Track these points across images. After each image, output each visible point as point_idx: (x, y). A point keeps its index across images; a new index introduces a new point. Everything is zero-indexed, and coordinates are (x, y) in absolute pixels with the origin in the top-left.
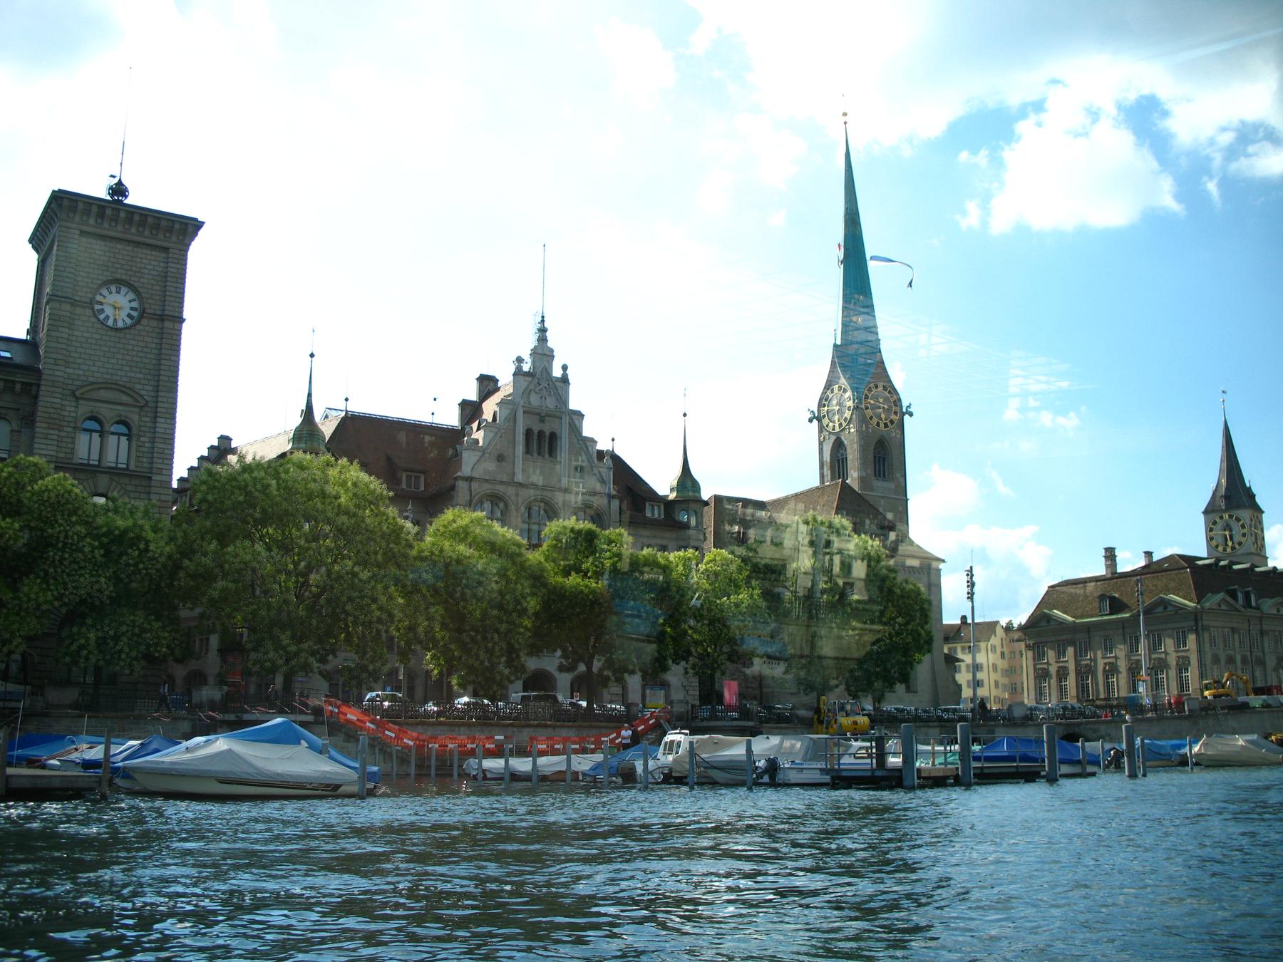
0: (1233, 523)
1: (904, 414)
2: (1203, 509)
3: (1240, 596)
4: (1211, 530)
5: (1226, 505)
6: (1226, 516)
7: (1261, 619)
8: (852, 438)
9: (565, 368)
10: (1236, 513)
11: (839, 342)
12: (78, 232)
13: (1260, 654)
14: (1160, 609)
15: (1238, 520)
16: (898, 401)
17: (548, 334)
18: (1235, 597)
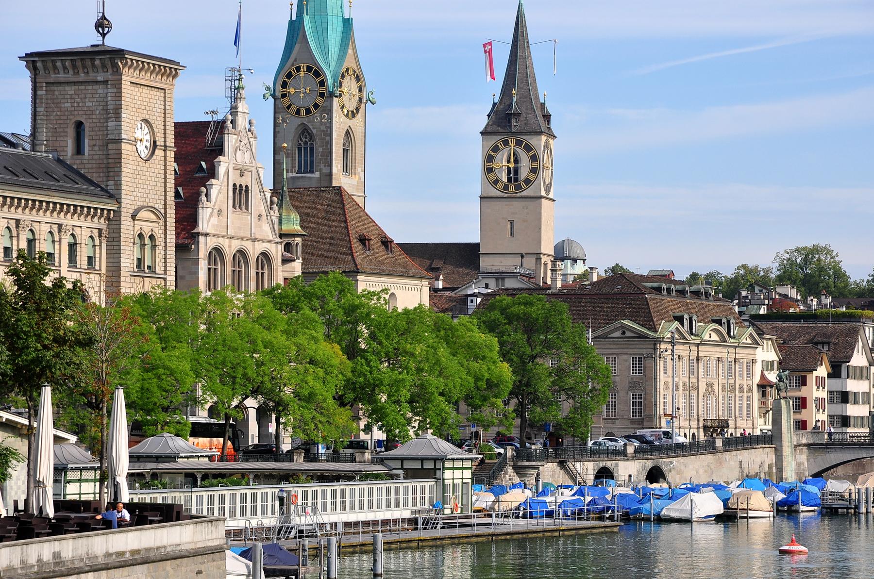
2: (482, 129)
4: (490, 159)
7: (698, 345)
8: (323, 128)
14: (618, 334)
15: (528, 148)
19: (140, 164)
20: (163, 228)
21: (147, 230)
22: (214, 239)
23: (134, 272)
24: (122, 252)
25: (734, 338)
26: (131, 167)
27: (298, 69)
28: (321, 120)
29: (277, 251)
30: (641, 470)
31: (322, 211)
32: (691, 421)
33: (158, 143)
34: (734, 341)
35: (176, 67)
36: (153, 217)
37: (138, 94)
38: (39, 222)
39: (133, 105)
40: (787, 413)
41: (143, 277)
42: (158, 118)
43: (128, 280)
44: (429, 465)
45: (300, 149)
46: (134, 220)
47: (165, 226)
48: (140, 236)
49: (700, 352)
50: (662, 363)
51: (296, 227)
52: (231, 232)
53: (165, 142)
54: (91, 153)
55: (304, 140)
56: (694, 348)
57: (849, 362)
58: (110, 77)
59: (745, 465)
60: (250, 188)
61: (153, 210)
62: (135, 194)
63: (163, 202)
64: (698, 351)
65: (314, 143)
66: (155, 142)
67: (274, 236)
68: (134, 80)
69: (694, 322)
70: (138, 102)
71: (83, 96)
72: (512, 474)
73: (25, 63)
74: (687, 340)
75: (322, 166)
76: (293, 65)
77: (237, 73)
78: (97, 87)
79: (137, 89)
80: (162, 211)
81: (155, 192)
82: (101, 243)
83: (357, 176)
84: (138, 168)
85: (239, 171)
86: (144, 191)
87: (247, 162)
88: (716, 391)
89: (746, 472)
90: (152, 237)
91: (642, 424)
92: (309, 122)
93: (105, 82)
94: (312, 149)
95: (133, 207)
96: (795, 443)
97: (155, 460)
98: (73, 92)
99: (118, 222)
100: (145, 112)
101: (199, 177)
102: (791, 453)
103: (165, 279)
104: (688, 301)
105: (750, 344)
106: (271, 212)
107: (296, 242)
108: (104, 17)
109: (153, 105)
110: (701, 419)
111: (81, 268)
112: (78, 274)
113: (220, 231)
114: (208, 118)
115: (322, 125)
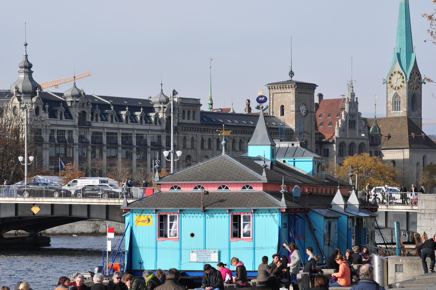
1: (422, 83)
8: (404, 94)
9: (357, 98)
16: (420, 78)
22: (342, 139)
27: (395, 73)
31: (399, 125)
37: (301, 96)
39: (299, 99)
52: (348, 137)
55: (397, 98)
58: (291, 91)
60: (356, 121)
61: (307, 132)
66: (308, 111)
68: (299, 91)
70: (301, 98)
71: (284, 97)
75: (403, 108)
76: (393, 71)
79: (301, 94)
87: (355, 112)
92: (399, 92)
100: (304, 101)
101: (337, 118)
108: (291, 71)
109: (307, 99)
114: (341, 97)
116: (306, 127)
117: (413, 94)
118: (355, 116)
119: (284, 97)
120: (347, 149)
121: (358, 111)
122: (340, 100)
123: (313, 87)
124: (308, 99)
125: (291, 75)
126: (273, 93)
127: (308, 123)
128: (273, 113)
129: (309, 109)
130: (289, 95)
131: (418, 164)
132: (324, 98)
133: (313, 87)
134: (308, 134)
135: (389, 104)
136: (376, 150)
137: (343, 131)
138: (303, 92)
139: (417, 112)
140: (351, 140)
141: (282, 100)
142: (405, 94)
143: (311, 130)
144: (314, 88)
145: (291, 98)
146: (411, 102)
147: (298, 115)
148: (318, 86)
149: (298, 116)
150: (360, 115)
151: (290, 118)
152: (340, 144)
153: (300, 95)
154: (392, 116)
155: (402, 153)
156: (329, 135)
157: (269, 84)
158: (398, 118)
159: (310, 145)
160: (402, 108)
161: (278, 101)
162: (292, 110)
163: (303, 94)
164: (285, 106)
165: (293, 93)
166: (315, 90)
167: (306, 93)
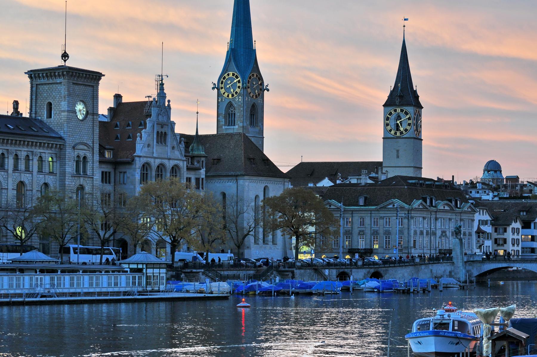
0: (402, 115)
1: (265, 90)
2: (384, 103)
3: (428, 201)
4: (388, 119)
5: (400, 102)
6: (399, 110)
7: (436, 212)
8: (240, 104)
9: (169, 101)
10: (406, 108)
11: (233, 47)
12: (72, 84)
13: (434, 230)
14: (391, 206)
16: (262, 84)
17: (164, 86)
18: (426, 202)
19: (79, 122)
20: (92, 153)
21: (82, 154)
23: (74, 174)
24: (67, 164)
25: (460, 208)
26: (73, 124)
28: (239, 100)
29: (183, 165)
30: (367, 273)
31: (233, 145)
32: (431, 250)
33: (89, 112)
34: (460, 210)
35: (99, 75)
36: (85, 148)
38: (21, 150)
39: (74, 94)
40: (460, 245)
41: (79, 177)
42: (90, 100)
43: (70, 178)
44: (140, 266)
45: (229, 114)
46: (74, 149)
47: (93, 152)
48: (78, 157)
49: (437, 216)
50: (412, 221)
51: (202, 153)
52: (155, 155)
53: (93, 111)
54: (55, 117)
55: (231, 109)
56: (433, 213)
57: (534, 221)
58: (63, 81)
59: (434, 271)
60: (167, 133)
61: (85, 144)
62: (75, 137)
63: (92, 140)
64: (436, 215)
65: (236, 111)
67: (182, 157)
69: (434, 201)
71: (51, 90)
72: (276, 274)
73: (28, 75)
74: (427, 209)
75: (239, 122)
77: (161, 77)
78: (57, 86)
79: (77, 86)
80: (92, 145)
81: (87, 136)
82: (57, 160)
83: (259, 128)
84: (77, 124)
85: (160, 126)
86: (80, 135)
88: (448, 235)
89: (435, 275)
90: (85, 158)
91: (402, 251)
93: (61, 83)
94: (235, 114)
95: (74, 143)
96: (465, 260)
97: (26, 263)
98: (47, 88)
99: (65, 150)
102: (463, 265)
103: (92, 178)
104: (433, 190)
105: (470, 211)
106: (181, 146)
107: (202, 160)
108: (65, 52)
110: (438, 249)
111: (45, 173)
112: (43, 176)
113: (149, 155)
114: (147, 99)
115: (239, 102)
116: (85, 136)
117: (252, 104)
118: (167, 126)
119: (51, 90)
120: (154, 173)
121: (170, 119)
122: (145, 102)
123: (96, 77)
124: (89, 94)
125: (65, 58)
126: (36, 84)
127: (88, 129)
128: (36, 114)
129: (91, 110)
130: (59, 88)
131: (257, 197)
132: (124, 100)
133: (96, 77)
134: (87, 146)
135: (221, 116)
136: (197, 176)
137: (148, 147)
138: (80, 83)
139: (257, 129)
140: (159, 160)
141: (48, 94)
142: (242, 103)
143: (93, 142)
144: (98, 77)
145: (62, 91)
146: (249, 115)
147: (71, 117)
148: (104, 75)
149: (73, 119)
150: (173, 124)
151: (60, 121)
152: (143, 165)
153: (77, 87)
154: (224, 132)
155: (234, 182)
156: (128, 152)
157: (31, 71)
158: (231, 135)
159: (90, 163)
160: (237, 123)
161: (43, 97)
162: (63, 109)
163: (81, 87)
164: (53, 104)
165: (64, 83)
166: (100, 82)
167: (86, 85)
